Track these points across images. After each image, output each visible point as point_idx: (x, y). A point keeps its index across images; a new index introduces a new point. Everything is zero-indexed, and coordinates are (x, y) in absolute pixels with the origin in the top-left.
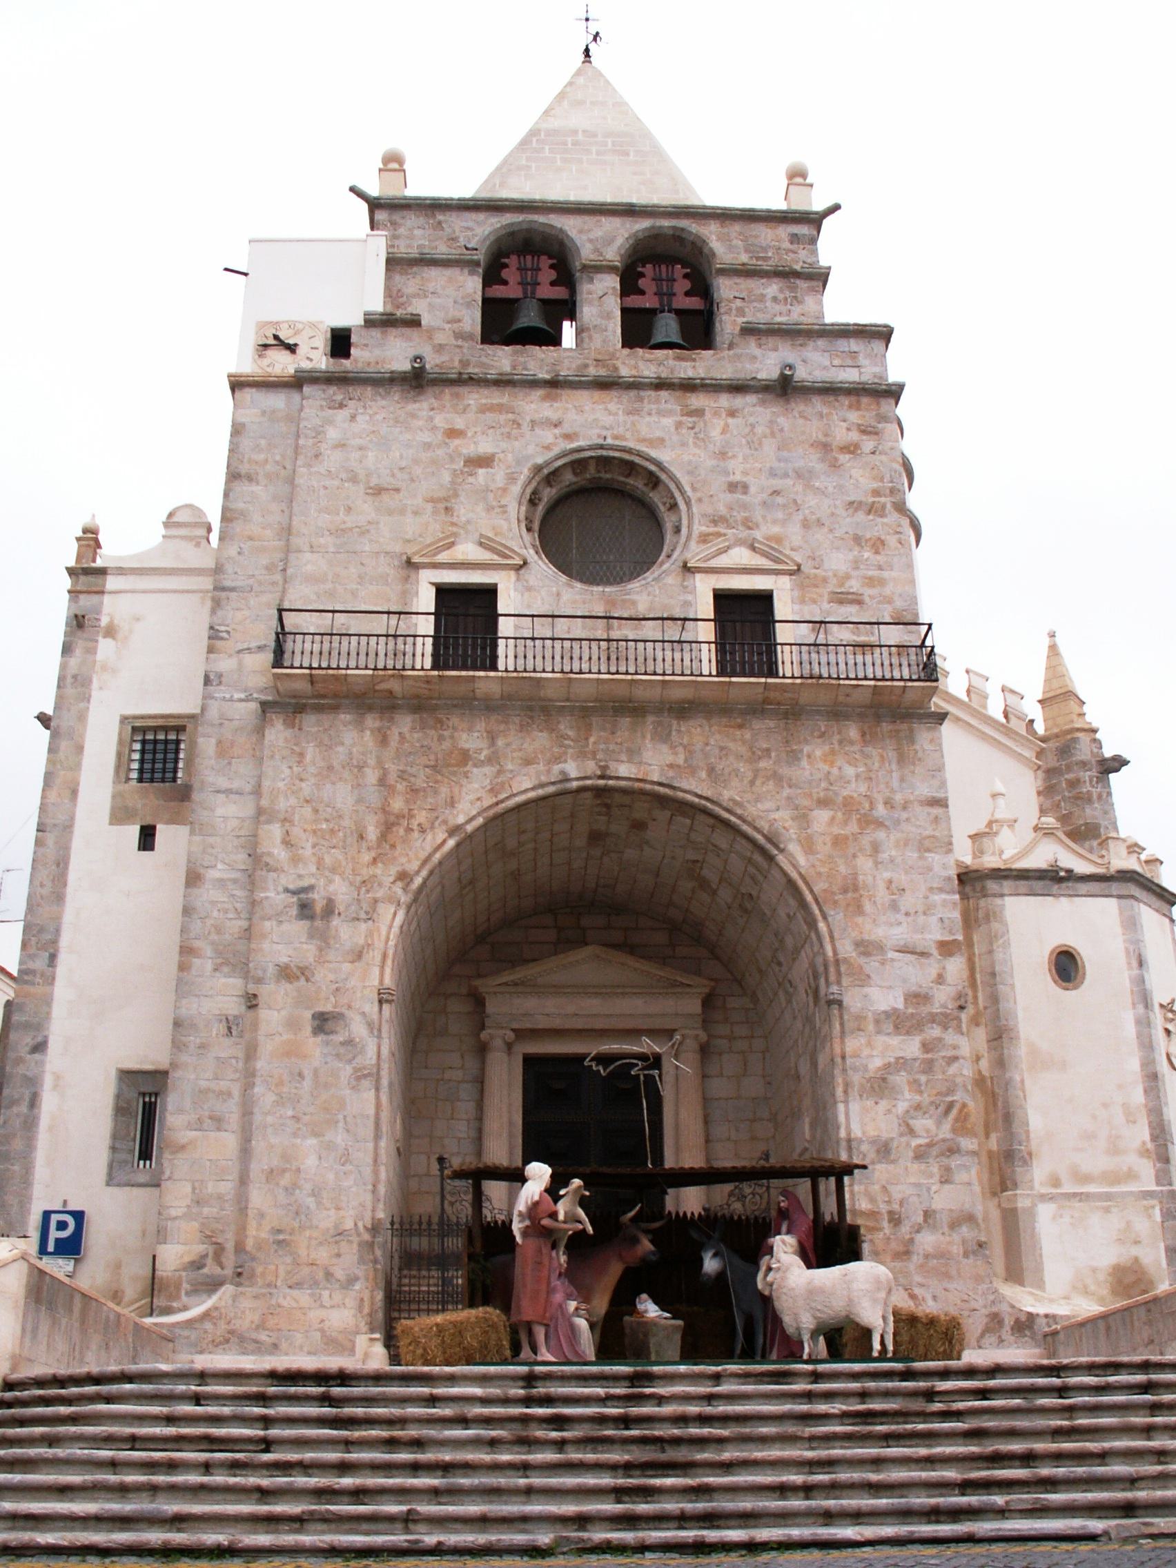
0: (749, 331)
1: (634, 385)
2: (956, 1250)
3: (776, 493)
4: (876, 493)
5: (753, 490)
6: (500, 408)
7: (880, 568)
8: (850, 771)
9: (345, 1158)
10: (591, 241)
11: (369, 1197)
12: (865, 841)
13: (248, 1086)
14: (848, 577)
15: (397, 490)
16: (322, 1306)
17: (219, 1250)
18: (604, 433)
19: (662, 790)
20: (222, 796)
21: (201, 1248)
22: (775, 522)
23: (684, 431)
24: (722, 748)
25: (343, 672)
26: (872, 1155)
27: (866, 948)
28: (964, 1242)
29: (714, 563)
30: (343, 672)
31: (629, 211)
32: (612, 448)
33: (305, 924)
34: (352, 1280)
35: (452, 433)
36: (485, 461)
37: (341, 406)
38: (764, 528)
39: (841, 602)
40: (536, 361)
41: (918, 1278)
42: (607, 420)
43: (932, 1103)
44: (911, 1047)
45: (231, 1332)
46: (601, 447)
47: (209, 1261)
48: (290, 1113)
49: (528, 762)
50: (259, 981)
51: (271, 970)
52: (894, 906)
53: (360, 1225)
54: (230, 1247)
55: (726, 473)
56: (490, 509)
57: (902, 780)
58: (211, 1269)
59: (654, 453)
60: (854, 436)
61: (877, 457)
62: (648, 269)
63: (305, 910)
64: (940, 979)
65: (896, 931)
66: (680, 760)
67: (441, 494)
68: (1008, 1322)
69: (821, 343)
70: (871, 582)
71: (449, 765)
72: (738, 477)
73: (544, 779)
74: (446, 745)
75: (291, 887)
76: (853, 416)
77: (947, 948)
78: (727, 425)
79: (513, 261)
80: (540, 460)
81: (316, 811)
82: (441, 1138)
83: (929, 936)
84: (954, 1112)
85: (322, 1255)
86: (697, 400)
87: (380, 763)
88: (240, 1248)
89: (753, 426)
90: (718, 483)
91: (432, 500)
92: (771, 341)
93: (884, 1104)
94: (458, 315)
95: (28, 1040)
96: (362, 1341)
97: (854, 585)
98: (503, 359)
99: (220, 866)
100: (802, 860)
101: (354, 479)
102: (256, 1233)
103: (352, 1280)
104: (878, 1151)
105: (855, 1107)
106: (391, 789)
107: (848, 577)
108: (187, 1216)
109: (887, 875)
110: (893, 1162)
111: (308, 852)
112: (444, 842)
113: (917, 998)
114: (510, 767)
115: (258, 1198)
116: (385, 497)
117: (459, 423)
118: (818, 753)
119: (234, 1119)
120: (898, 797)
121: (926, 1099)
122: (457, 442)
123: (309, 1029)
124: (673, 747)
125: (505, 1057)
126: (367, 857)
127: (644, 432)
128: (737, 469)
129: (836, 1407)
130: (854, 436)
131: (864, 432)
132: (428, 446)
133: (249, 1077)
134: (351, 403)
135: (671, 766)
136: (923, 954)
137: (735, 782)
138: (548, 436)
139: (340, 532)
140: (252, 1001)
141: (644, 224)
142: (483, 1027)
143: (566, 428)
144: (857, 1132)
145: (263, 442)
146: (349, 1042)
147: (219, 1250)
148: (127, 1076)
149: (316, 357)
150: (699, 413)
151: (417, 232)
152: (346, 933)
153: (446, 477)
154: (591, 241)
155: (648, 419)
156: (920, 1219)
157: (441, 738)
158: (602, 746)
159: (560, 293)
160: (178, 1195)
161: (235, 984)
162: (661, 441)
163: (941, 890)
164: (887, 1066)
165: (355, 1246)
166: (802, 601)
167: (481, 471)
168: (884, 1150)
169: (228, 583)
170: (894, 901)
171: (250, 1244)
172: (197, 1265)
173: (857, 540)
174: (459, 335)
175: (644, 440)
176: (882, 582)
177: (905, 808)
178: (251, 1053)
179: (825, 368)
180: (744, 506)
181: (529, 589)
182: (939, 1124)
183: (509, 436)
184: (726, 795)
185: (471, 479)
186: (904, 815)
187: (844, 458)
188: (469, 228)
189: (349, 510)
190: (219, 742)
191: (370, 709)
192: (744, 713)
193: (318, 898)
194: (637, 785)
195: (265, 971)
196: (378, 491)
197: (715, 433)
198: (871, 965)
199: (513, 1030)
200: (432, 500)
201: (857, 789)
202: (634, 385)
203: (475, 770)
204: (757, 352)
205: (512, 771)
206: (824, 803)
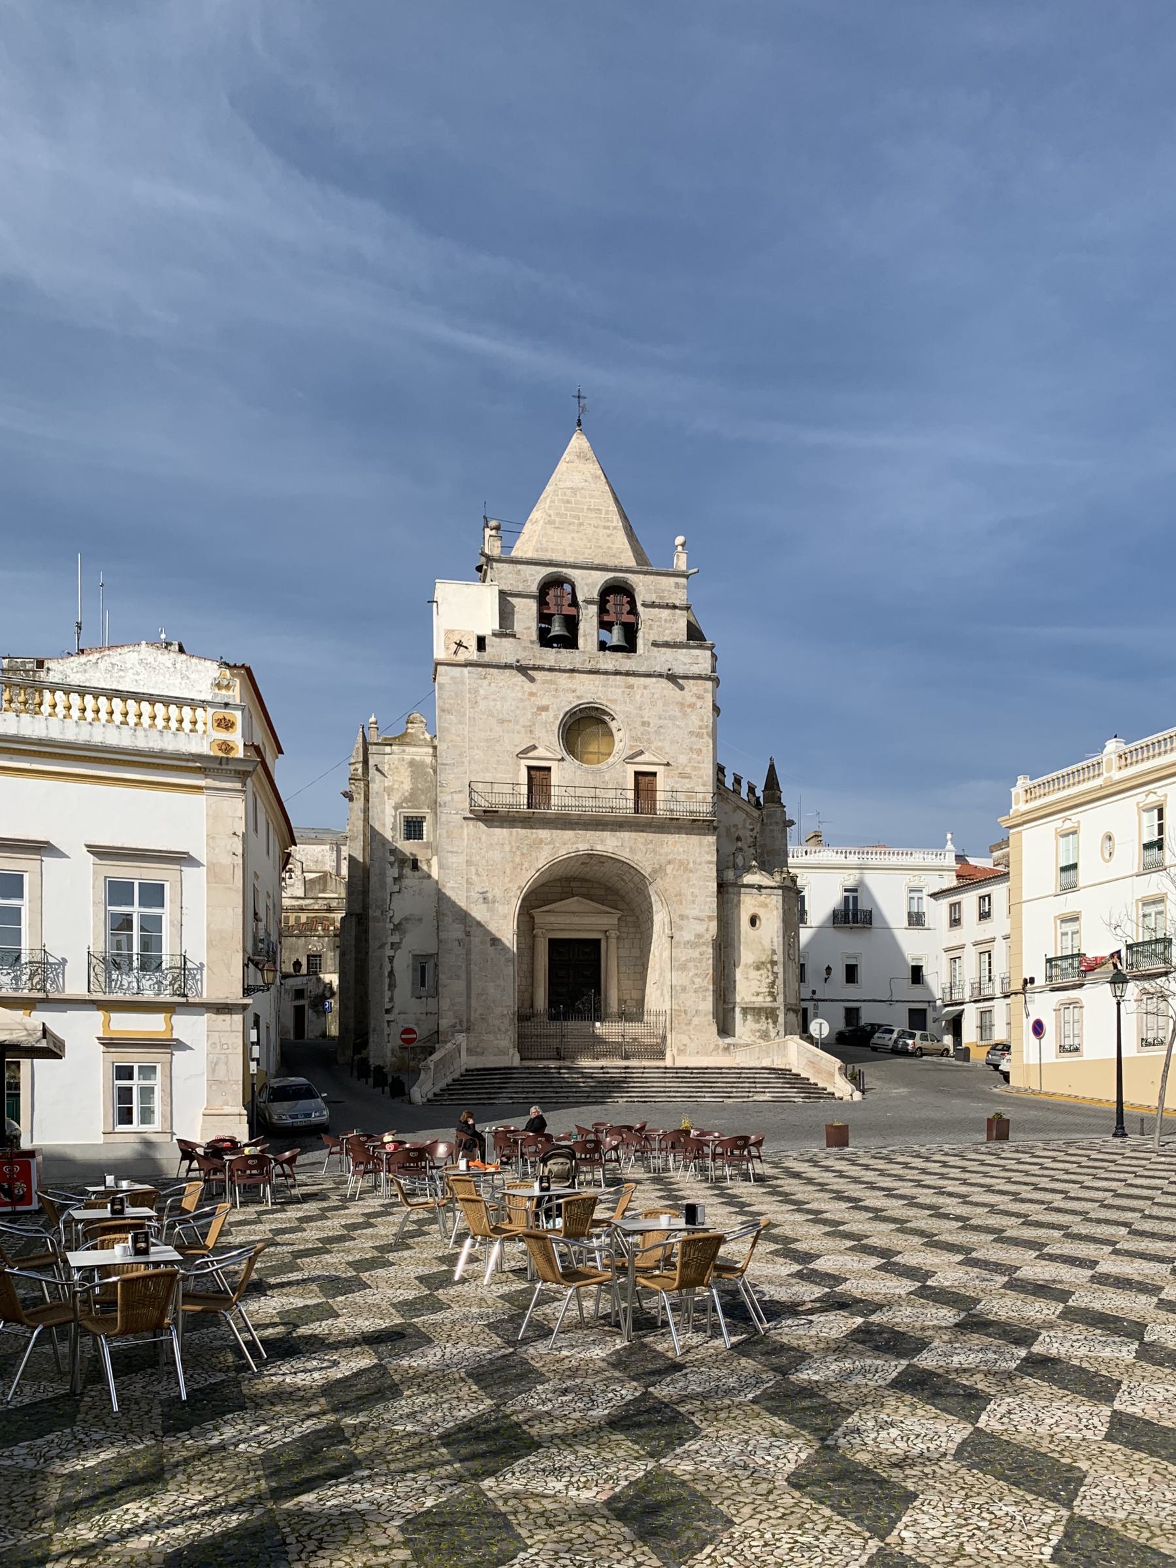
0: (655, 644)
1: (606, 673)
2: (706, 1023)
3: (661, 727)
4: (701, 727)
5: (651, 725)
6: (551, 682)
7: (699, 763)
8: (681, 850)
10: (586, 584)
11: (512, 1004)
12: (685, 877)
13: (468, 965)
14: (686, 766)
15: (510, 721)
17: (461, 1021)
19: (613, 856)
20: (450, 854)
21: (454, 1021)
22: (660, 740)
27: (682, 917)
29: (635, 760)
31: (605, 569)
33: (485, 905)
34: (507, 1030)
35: (532, 694)
36: (545, 708)
37: (485, 678)
39: (683, 777)
40: (564, 657)
41: (693, 1032)
42: (594, 689)
44: (695, 954)
49: (565, 844)
50: (471, 927)
54: (465, 1019)
55: (642, 717)
56: (547, 731)
57: (700, 853)
58: (458, 1027)
59: (613, 707)
61: (703, 710)
62: (611, 598)
63: (484, 899)
64: (707, 930)
65: (693, 911)
68: (721, 1047)
69: (684, 650)
70: (695, 768)
72: (646, 719)
73: (570, 851)
74: (534, 836)
76: (694, 689)
78: (643, 693)
79: (552, 592)
80: (568, 709)
81: (487, 861)
85: (497, 1022)
86: (631, 680)
87: (510, 843)
88: (468, 1021)
89: (653, 694)
91: (524, 726)
92: (663, 650)
94: (530, 625)
95: (377, 944)
96: (511, 1051)
97: (688, 770)
98: (551, 656)
101: (493, 716)
103: (507, 1030)
106: (514, 853)
107: (686, 766)
108: (449, 1010)
111: (485, 878)
113: (699, 936)
115: (474, 1002)
116: (506, 724)
117: (535, 691)
118: (670, 843)
119: (464, 976)
120: (698, 860)
122: (533, 699)
124: (618, 838)
126: (507, 880)
127: (610, 697)
128: (647, 715)
129: (671, 1075)
130: (694, 700)
131: (698, 698)
132: (522, 700)
133: (468, 961)
134: (489, 677)
136: (702, 920)
137: (639, 853)
138: (570, 697)
139: (487, 740)
140: (468, 934)
141: (612, 575)
142: (533, 929)
143: (578, 693)
145: (453, 694)
147: (461, 1021)
148: (415, 956)
149: (472, 654)
150: (631, 687)
151: (510, 576)
152: (502, 909)
153: (529, 716)
154: (586, 584)
155: (610, 690)
159: (572, 611)
160: (445, 1004)
161: (461, 926)
162: (616, 701)
163: (711, 896)
166: (668, 777)
167: (543, 713)
168: (684, 989)
169: (444, 762)
171: (472, 1019)
172: (454, 1026)
173: (691, 749)
174: (532, 642)
175: (608, 700)
178: (469, 952)
179: (685, 664)
180: (649, 733)
181: (564, 769)
183: (554, 696)
184: (636, 858)
187: (689, 710)
188: (533, 575)
189: (491, 730)
190: (447, 832)
191: (506, 821)
192: (643, 826)
193: (490, 896)
194: (605, 854)
197: (638, 697)
198: (685, 922)
200: (524, 726)
201: (683, 857)
202: (606, 673)
204: (657, 655)
206: (669, 863)
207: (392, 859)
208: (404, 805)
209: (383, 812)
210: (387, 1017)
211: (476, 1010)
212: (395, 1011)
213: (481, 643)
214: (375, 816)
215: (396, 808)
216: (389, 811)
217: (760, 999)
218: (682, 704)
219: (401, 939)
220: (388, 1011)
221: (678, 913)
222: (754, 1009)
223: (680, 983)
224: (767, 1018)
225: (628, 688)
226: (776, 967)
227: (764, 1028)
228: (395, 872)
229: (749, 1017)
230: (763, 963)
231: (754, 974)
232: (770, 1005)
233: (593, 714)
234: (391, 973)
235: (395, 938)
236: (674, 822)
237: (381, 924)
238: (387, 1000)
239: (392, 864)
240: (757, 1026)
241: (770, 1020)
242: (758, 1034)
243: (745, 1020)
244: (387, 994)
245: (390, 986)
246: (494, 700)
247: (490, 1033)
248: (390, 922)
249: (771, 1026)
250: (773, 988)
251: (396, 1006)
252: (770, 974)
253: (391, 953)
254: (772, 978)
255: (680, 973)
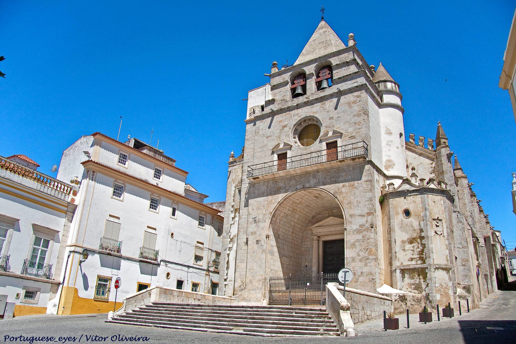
2: (367, 281)
4: (360, 111)
5: (334, 118)
9: (260, 267)
16: (256, 293)
18: (306, 114)
23: (321, 108)
24: (325, 177)
25: (257, 176)
26: (351, 261)
27: (351, 216)
28: (369, 279)
30: (257, 176)
32: (308, 116)
33: (255, 224)
35: (280, 121)
36: (285, 126)
38: (336, 126)
43: (364, 249)
44: (360, 237)
45: (244, 298)
46: (306, 117)
47: (242, 286)
48: (252, 259)
49: (291, 187)
51: (250, 233)
52: (358, 206)
53: (262, 278)
58: (242, 287)
60: (355, 99)
66: (317, 181)
67: (278, 135)
70: (357, 132)
71: (277, 190)
74: (277, 186)
75: (253, 217)
77: (369, 214)
82: (307, 259)
83: (365, 212)
84: (368, 250)
85: (257, 284)
90: (328, 119)
93: (354, 250)
97: (354, 134)
99: (244, 215)
100: (339, 199)
102: (248, 280)
104: (352, 260)
105: (348, 250)
109: (357, 199)
110: (355, 262)
112: (277, 205)
113: (361, 226)
114: (287, 188)
117: (281, 119)
121: (363, 247)
123: (255, 242)
125: (317, 241)
130: (355, 99)
135: (315, 183)
144: (348, 256)
146: (262, 245)
152: (261, 225)
153: (279, 131)
156: (360, 274)
157: (277, 185)
158: (303, 181)
164: (355, 241)
165: (262, 282)
168: (353, 259)
170: (358, 205)
176: (360, 132)
177: (361, 184)
182: (365, 254)
185: (283, 131)
186: (361, 185)
187: (353, 105)
193: (257, 219)
195: (249, 233)
196: (267, 137)
199: (317, 236)
203: (282, 190)
205: (288, 189)
207: (232, 209)
208: (239, 185)
209: (231, 190)
210: (226, 283)
211: (248, 278)
212: (228, 280)
213: (263, 108)
214: (228, 192)
215: (235, 187)
216: (233, 189)
217: (414, 262)
218: (349, 103)
219: (233, 245)
220: (225, 280)
221: (350, 213)
222: (410, 269)
223: (351, 256)
224: (419, 276)
225: (322, 105)
226: (423, 241)
227: (417, 282)
228: (232, 215)
229: (406, 275)
230: (414, 239)
231: (408, 246)
232: (420, 266)
233: (310, 123)
234: (228, 262)
235: (230, 246)
236: (343, 163)
237: (226, 239)
238: (225, 275)
239: (232, 212)
240: (412, 281)
241: (421, 277)
242: (413, 286)
243: (403, 277)
244: (226, 272)
245: (227, 268)
246: (265, 129)
247: (253, 290)
248: (230, 238)
249: (422, 280)
250: (422, 254)
251: (228, 277)
252: (419, 245)
253: (228, 252)
254: (421, 248)
255: (351, 250)
